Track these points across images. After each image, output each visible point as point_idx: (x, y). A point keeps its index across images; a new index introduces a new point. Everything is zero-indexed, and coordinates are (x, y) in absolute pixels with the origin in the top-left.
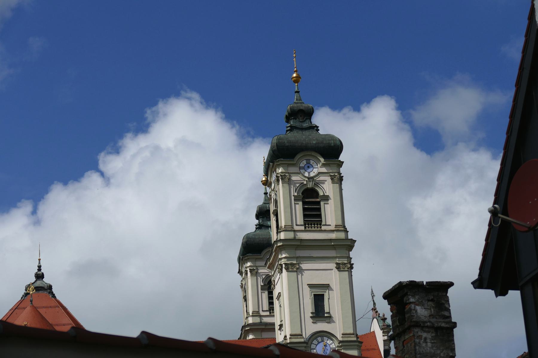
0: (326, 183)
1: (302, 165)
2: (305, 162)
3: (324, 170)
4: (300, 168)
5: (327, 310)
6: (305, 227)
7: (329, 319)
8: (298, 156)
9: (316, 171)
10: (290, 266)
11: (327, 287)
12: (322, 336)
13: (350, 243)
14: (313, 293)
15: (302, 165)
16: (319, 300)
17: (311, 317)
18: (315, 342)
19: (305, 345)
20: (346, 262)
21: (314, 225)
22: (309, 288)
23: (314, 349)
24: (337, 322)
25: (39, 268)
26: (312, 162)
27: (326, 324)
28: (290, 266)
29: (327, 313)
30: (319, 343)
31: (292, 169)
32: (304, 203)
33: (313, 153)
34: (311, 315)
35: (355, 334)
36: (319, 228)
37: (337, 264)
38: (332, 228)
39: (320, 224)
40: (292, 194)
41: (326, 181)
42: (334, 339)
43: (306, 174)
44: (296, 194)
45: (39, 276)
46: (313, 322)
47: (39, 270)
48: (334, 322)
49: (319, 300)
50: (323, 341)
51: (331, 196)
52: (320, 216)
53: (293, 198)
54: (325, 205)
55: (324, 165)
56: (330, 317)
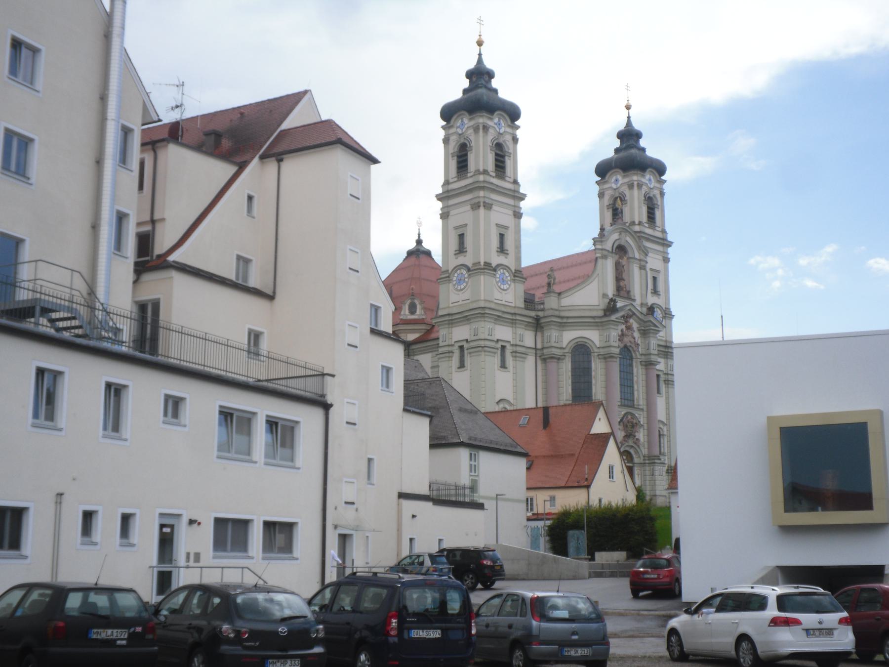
1: (458, 124)
2: (460, 121)
4: (457, 128)
6: (458, 178)
9: (466, 126)
19: (447, 279)
25: (419, 235)
45: (419, 242)
47: (419, 237)
53: (450, 156)
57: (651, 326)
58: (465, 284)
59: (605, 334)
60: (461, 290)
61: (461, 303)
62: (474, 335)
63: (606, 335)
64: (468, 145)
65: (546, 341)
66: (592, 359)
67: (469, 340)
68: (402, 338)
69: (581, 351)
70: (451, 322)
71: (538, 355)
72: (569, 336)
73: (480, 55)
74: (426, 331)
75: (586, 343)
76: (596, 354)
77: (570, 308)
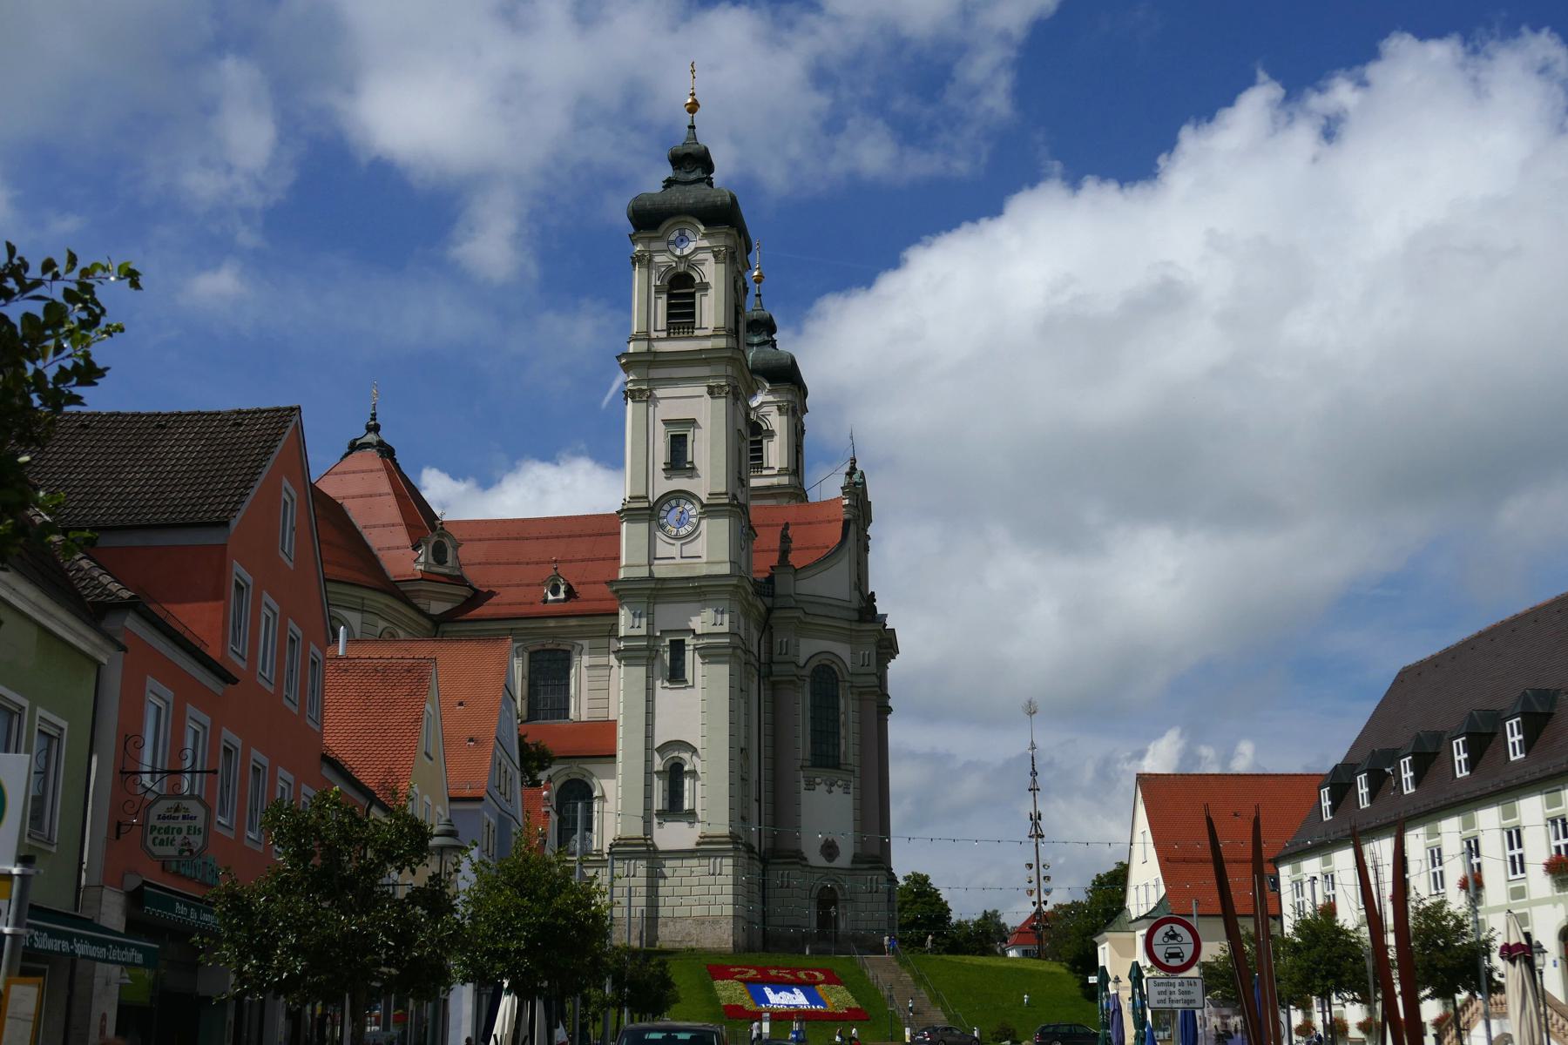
0: (707, 263)
1: (672, 238)
2: (677, 233)
3: (705, 243)
5: (689, 459)
6: (669, 334)
7: (691, 471)
8: (666, 224)
9: (692, 246)
10: (637, 394)
11: (692, 422)
12: (678, 498)
13: (730, 355)
14: (669, 434)
15: (672, 238)
16: (678, 444)
17: (664, 470)
18: (667, 507)
19: (649, 512)
20: (724, 384)
21: (683, 329)
22: (664, 427)
23: (664, 518)
24: (703, 476)
25: (374, 415)
26: (688, 233)
27: (686, 480)
28: (637, 394)
29: (689, 463)
30: (672, 508)
31: (655, 246)
32: (670, 296)
33: (689, 219)
34: (663, 467)
35: (730, 495)
36: (690, 334)
37: (709, 387)
38: (709, 332)
39: (693, 328)
40: (653, 284)
41: (707, 260)
42: (694, 501)
43: (678, 252)
44: (658, 283)
46: (666, 478)
48: (698, 476)
49: (678, 444)
50: (678, 506)
51: (712, 284)
52: (693, 315)
53: (653, 289)
54: (703, 298)
55: (705, 236)
56: (693, 469)
57: (886, 648)
58: (690, 529)
59: (862, 652)
60: (677, 538)
61: (679, 560)
62: (715, 624)
63: (864, 654)
64: (698, 280)
65: (777, 649)
66: (841, 692)
67: (698, 632)
68: (421, 606)
69: (825, 678)
70: (655, 592)
71: (762, 675)
72: (809, 648)
73: (692, 127)
74: (463, 599)
75: (834, 662)
76: (848, 684)
77: (812, 599)
